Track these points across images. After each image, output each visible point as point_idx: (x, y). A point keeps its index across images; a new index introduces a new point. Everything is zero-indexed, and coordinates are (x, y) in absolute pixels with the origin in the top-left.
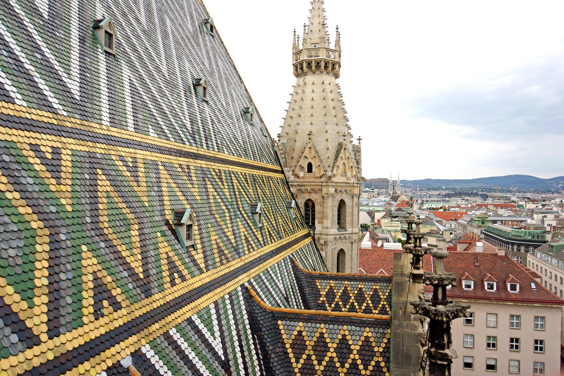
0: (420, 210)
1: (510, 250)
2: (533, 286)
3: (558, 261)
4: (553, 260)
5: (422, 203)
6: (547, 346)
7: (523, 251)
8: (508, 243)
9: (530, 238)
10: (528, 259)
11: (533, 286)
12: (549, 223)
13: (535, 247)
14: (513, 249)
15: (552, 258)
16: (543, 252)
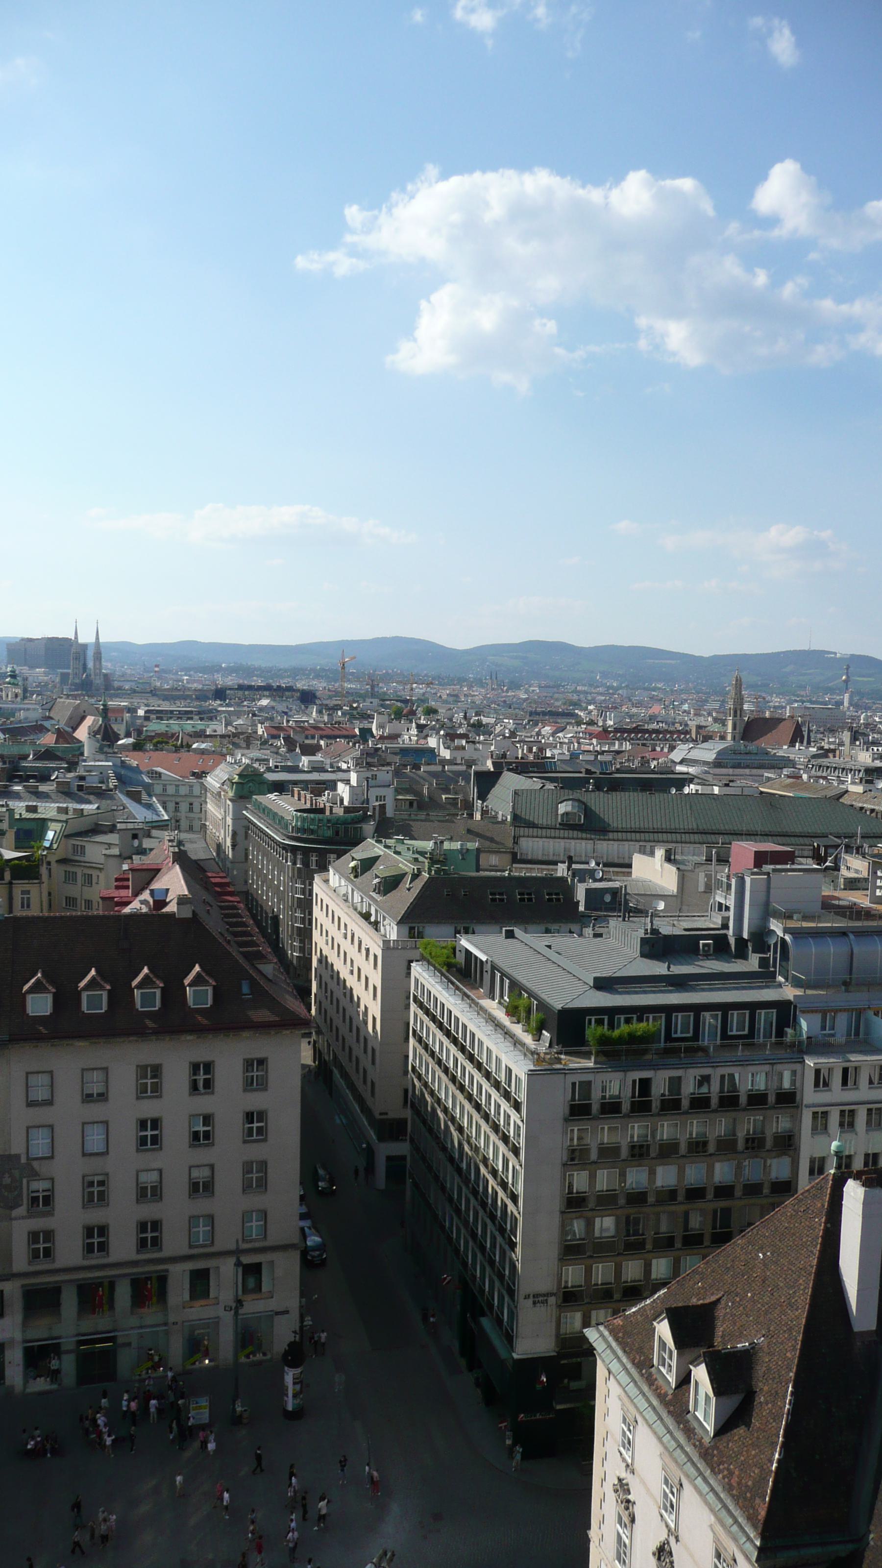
0: (102, 757)
1: (289, 863)
2: (245, 989)
3: (362, 898)
4: (355, 893)
5: (147, 718)
6: (273, 1121)
7: (314, 867)
8: (285, 847)
9: (329, 833)
10: (316, 889)
11: (245, 989)
12: (379, 794)
13: (340, 854)
14: (294, 863)
15: (353, 891)
16: (342, 875)
